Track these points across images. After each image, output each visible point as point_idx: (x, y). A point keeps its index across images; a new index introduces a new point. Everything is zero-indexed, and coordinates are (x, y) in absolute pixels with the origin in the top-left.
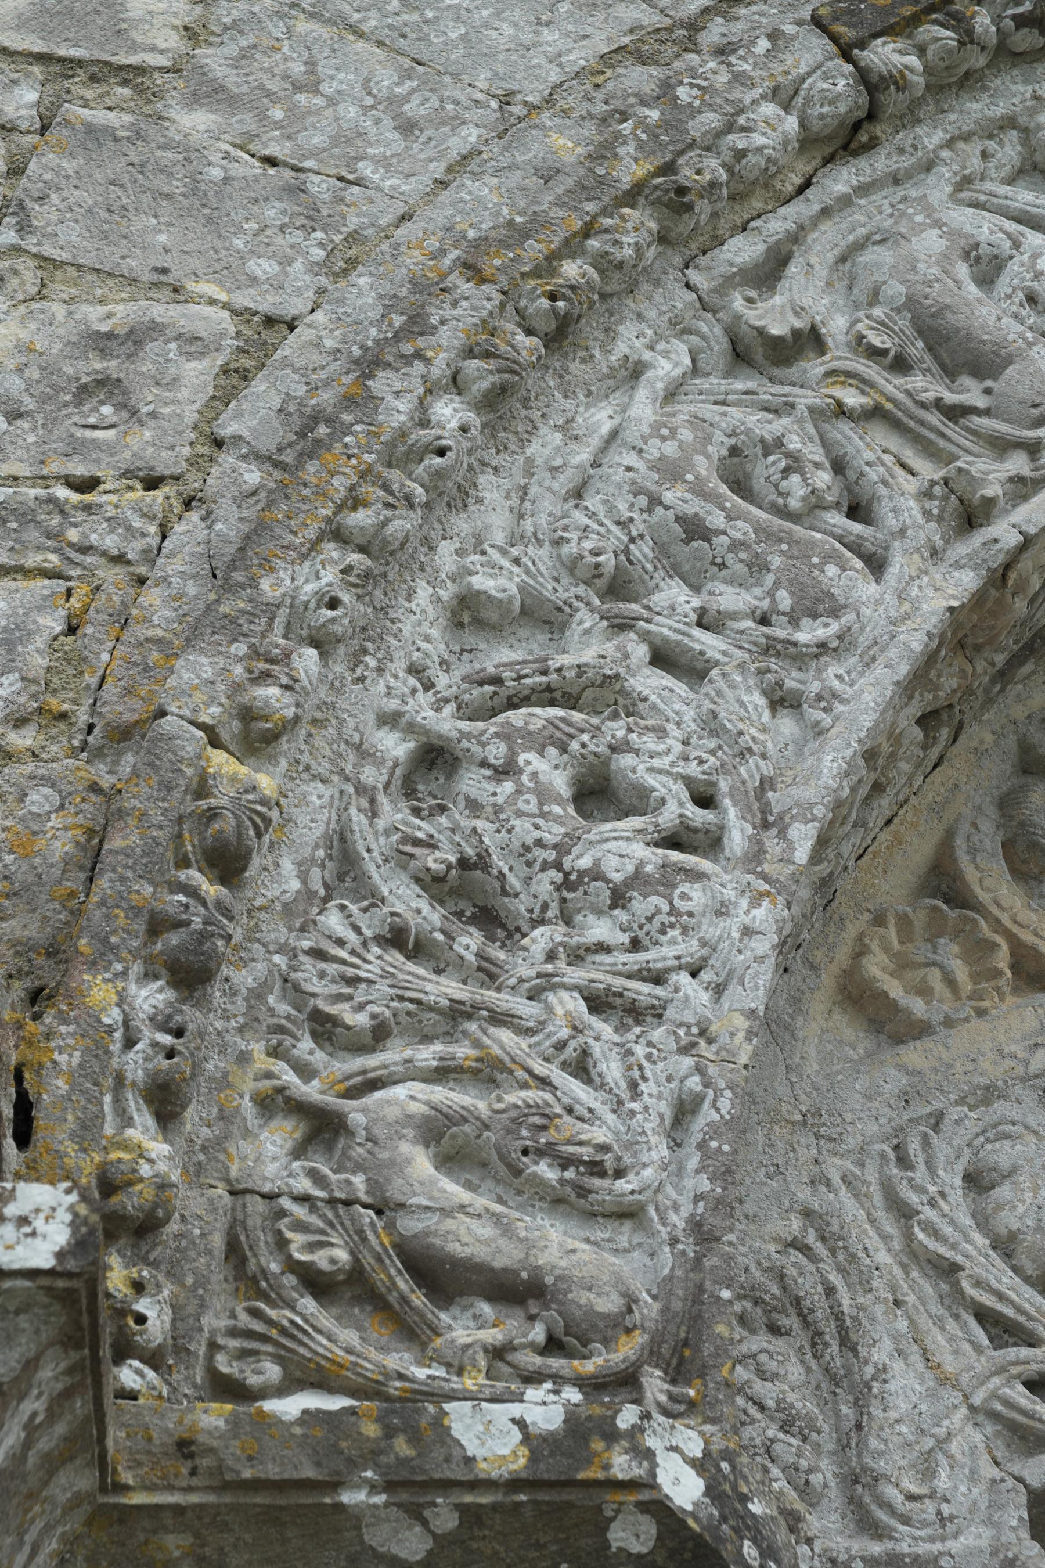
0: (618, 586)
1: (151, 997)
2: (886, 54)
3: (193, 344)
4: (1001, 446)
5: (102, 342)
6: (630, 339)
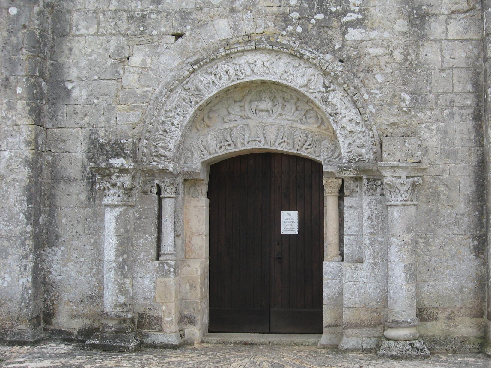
0: (176, 108)
1: (145, 141)
2: (195, 67)
3: (150, 92)
4: (200, 98)
5: (144, 92)
6: (177, 89)
